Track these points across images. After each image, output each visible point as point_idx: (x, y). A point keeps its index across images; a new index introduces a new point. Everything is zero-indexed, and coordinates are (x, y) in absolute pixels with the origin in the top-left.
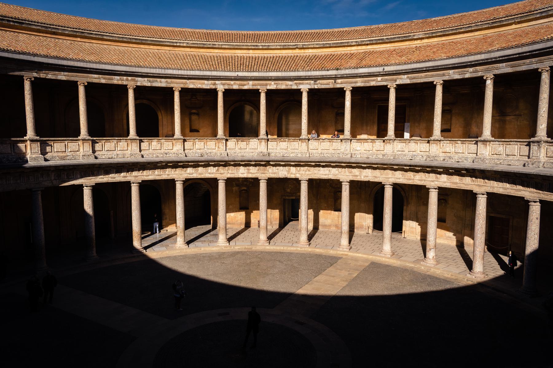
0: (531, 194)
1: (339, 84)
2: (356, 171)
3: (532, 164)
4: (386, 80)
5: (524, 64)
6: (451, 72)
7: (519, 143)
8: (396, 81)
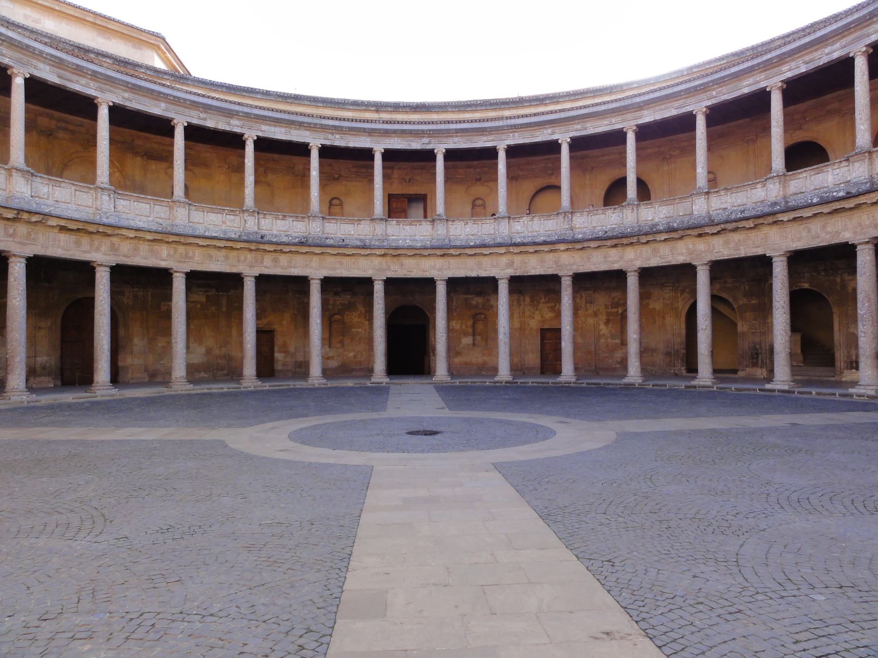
0: (108, 258)
3: (107, 218)
5: (77, 82)
7: (74, 188)
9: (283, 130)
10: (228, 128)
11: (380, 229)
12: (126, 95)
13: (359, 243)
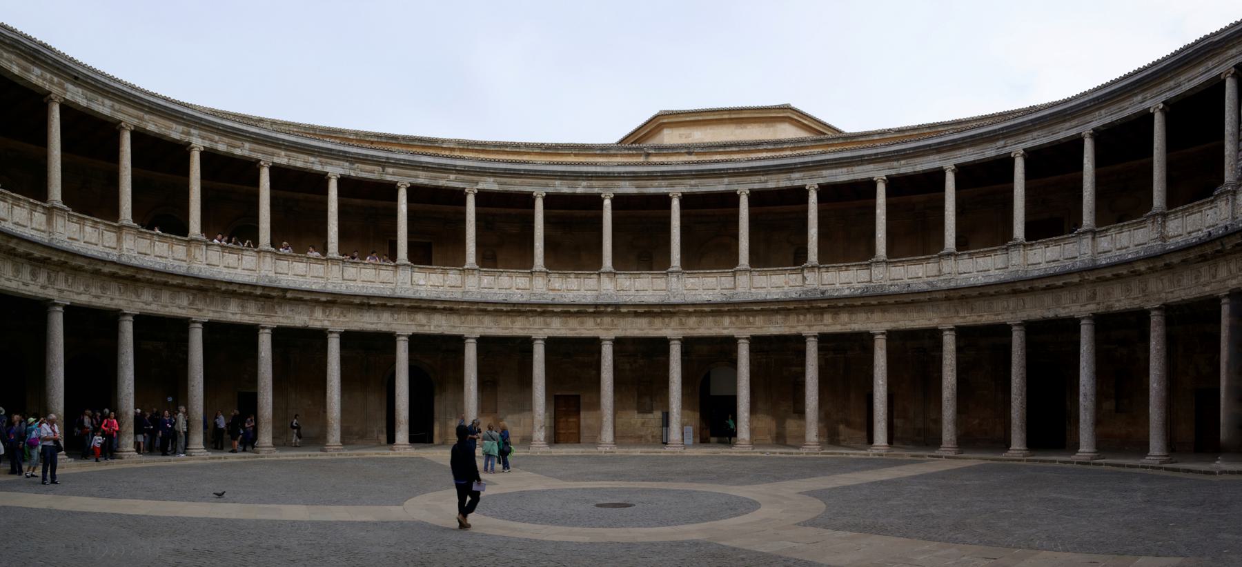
1: (390, 175)
2: (421, 318)
4: (462, 181)
5: (652, 186)
6: (557, 182)
8: (477, 183)
9: (845, 170)
10: (789, 184)
11: (948, 266)
12: (693, 182)
13: (925, 287)
